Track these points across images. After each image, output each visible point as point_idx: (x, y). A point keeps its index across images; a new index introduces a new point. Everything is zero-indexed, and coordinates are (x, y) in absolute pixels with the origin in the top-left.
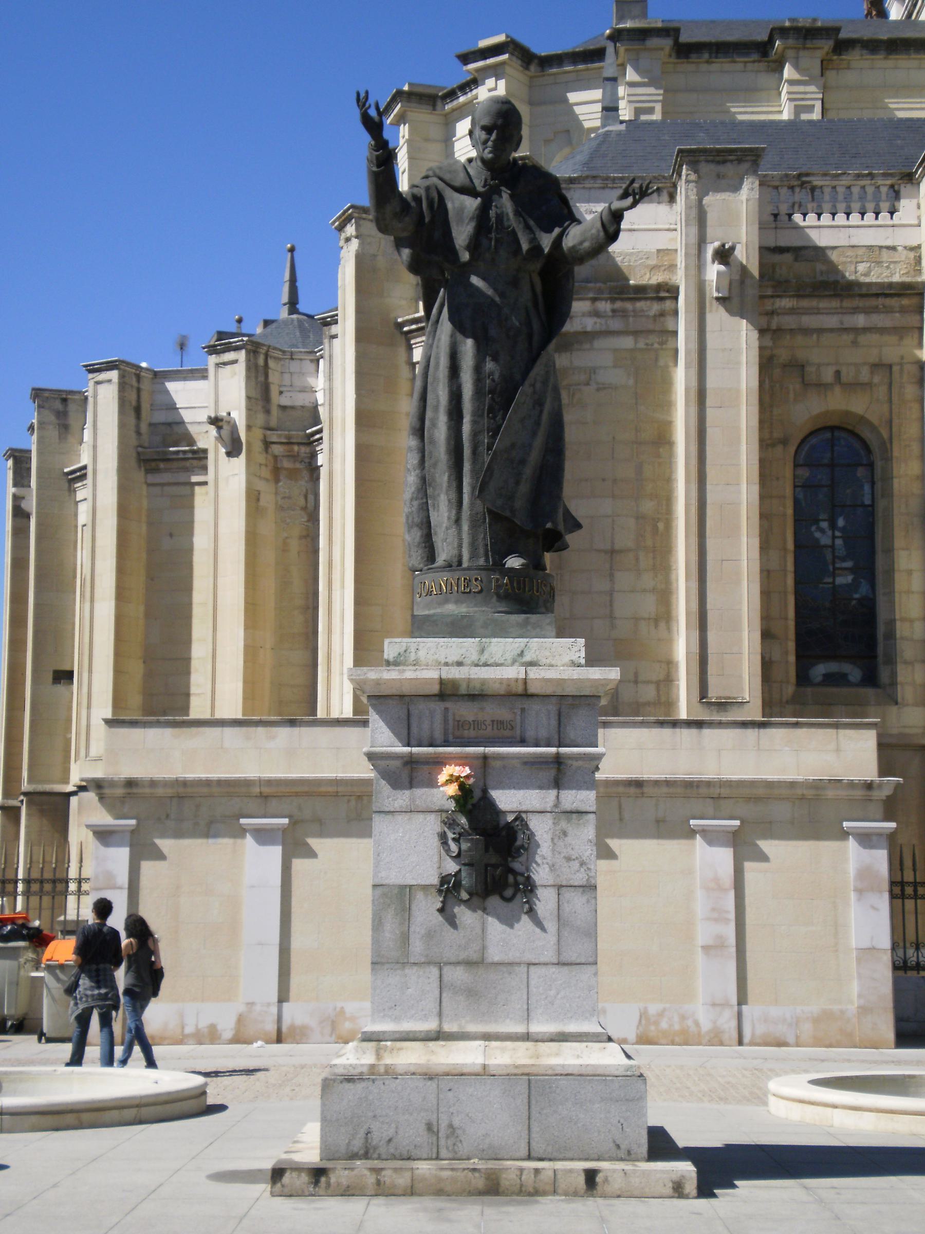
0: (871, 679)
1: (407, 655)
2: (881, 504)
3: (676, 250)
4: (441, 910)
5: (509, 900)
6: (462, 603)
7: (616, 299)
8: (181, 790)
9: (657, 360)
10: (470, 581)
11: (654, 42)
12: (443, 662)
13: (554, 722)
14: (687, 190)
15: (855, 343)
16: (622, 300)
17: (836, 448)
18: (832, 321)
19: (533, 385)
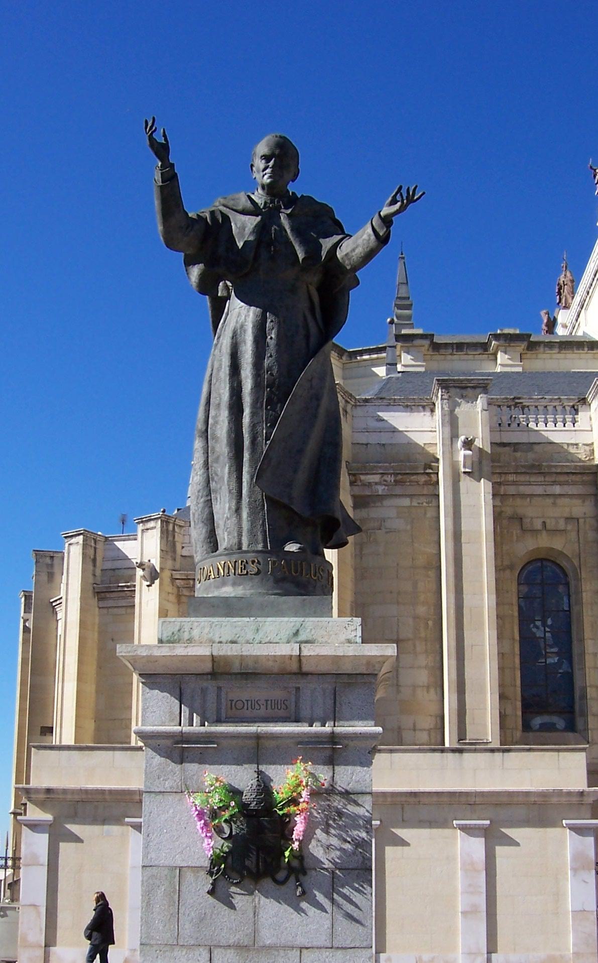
0: (571, 727)
2: (575, 609)
3: (436, 444)
4: (211, 892)
5: (282, 883)
8: (84, 796)
9: (425, 513)
10: (247, 562)
11: (418, 342)
13: (330, 702)
14: (442, 404)
15: (554, 504)
17: (545, 573)
18: (539, 490)
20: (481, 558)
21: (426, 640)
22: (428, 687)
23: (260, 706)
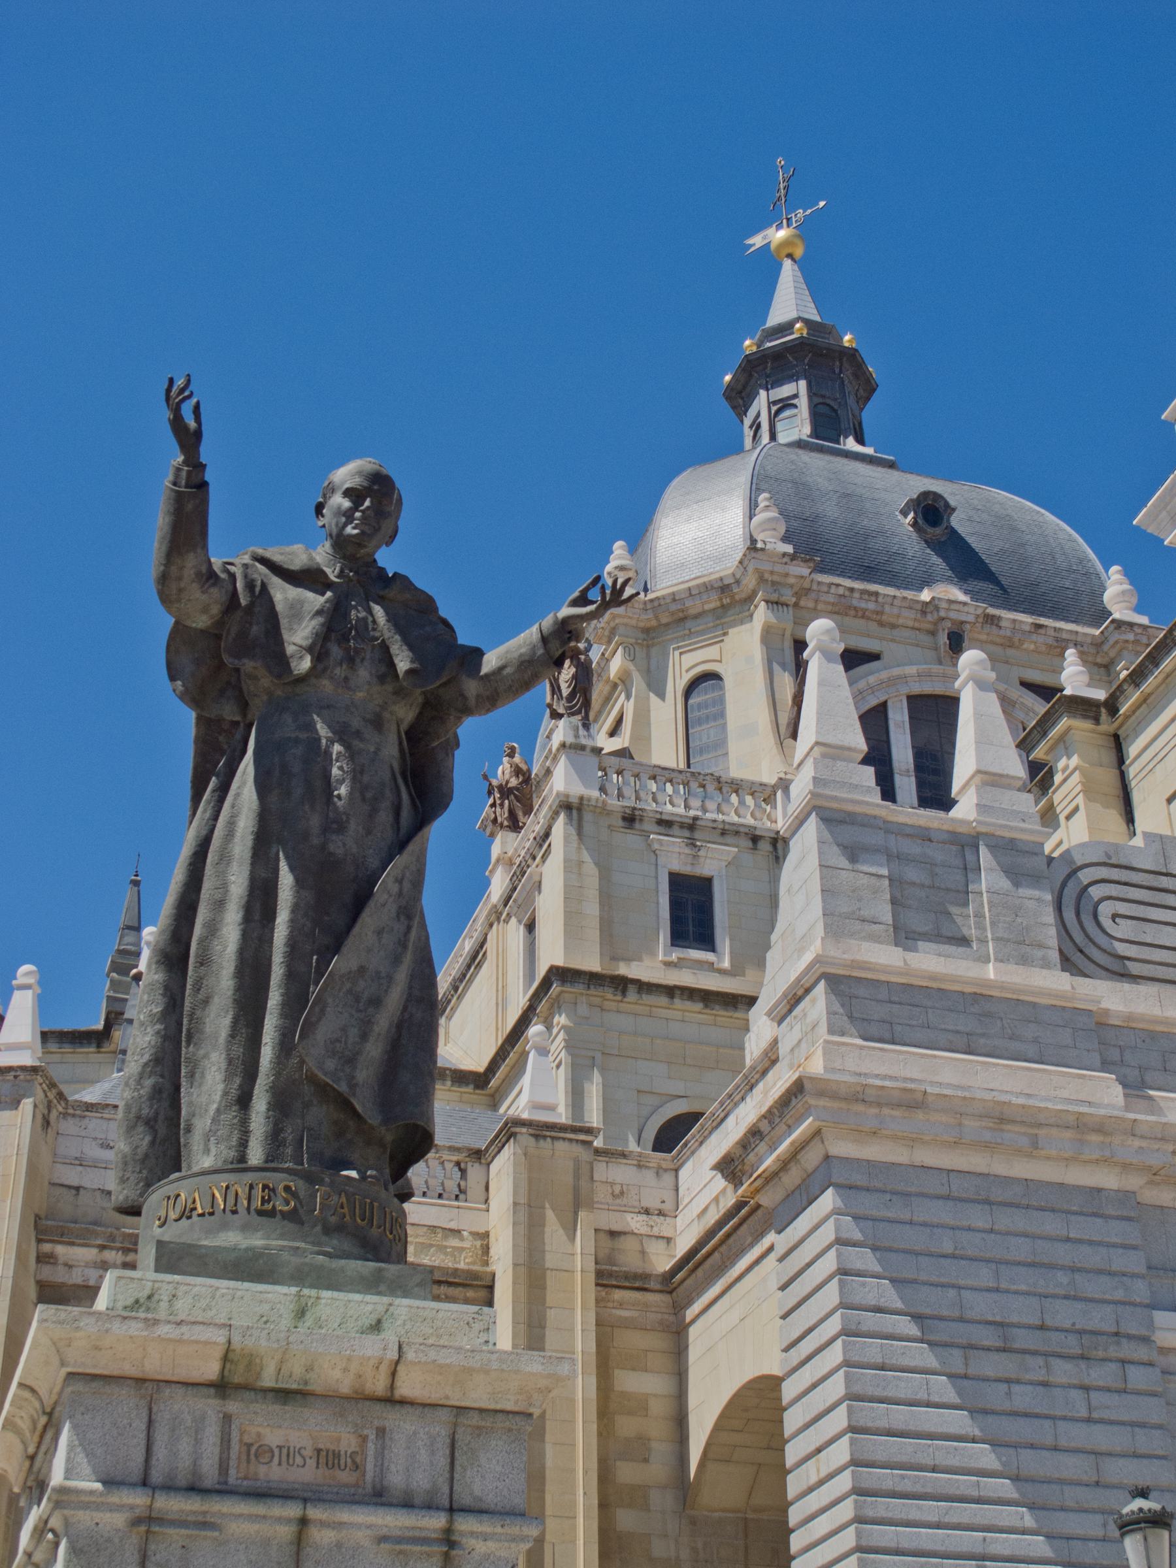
1: (152, 1305)
6: (256, 1230)
13: (442, 1461)
23: (305, 1461)
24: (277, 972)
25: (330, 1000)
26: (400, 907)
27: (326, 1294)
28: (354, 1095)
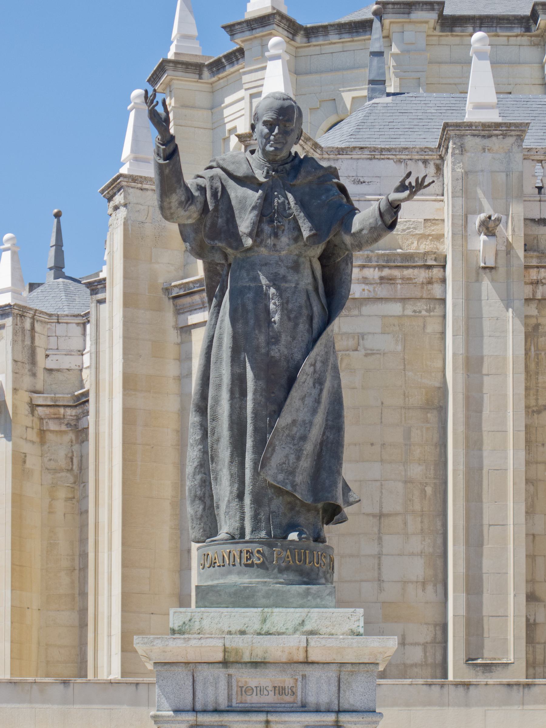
7: (384, 267)
9: (424, 327)
12: (226, 631)
13: (334, 689)
16: (390, 267)
19: (314, 365)
20: (505, 396)
21: (422, 516)
22: (424, 584)
24: (250, 428)
25: (277, 443)
26: (315, 379)
27: (276, 610)
28: (295, 491)
